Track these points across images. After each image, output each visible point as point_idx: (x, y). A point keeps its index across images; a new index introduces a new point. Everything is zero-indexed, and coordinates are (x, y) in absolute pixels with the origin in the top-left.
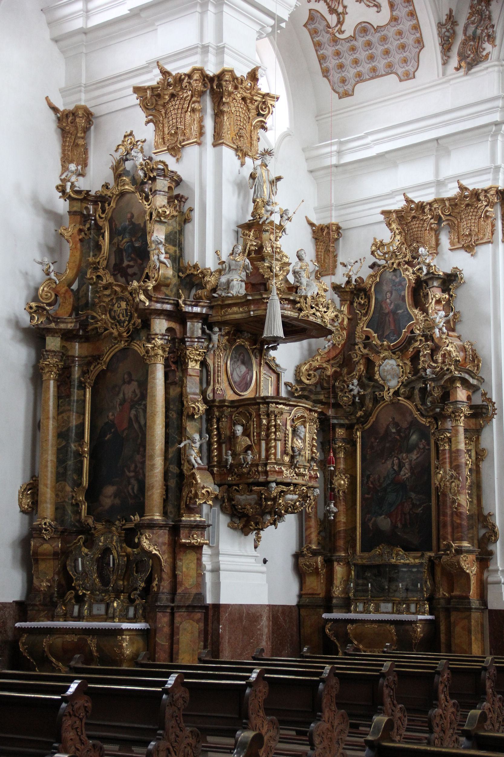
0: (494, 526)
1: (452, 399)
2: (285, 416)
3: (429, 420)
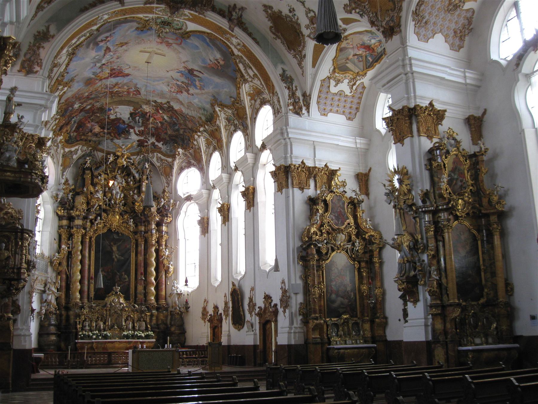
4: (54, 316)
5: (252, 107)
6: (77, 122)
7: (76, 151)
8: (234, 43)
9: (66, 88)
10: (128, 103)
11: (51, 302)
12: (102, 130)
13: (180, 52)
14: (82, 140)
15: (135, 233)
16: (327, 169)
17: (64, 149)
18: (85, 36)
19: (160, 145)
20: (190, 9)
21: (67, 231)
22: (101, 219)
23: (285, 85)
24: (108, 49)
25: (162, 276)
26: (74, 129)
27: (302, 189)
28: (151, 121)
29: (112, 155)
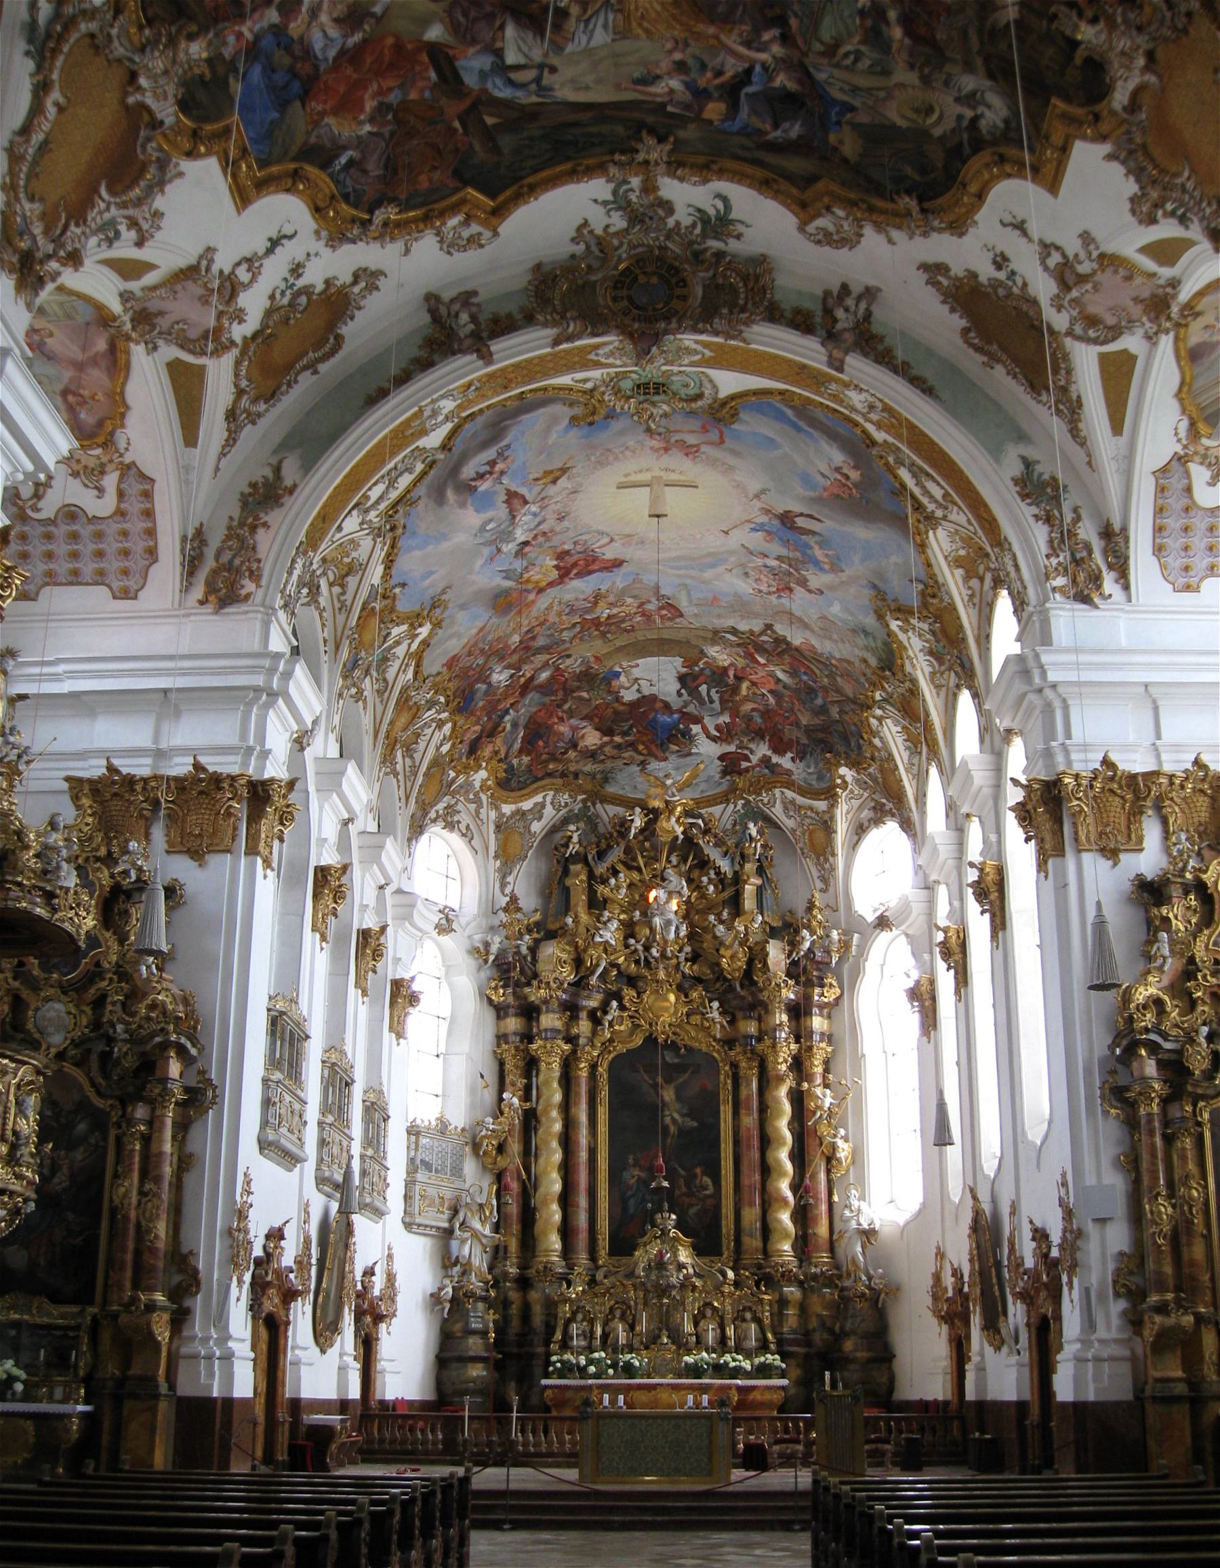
0: (196, 1272)
1: (158, 1074)
2: (8, 1078)
3: (110, 1102)
4: (480, 1305)
5: (976, 600)
6: (522, 722)
7: (539, 809)
8: (859, 406)
9: (424, 631)
10: (662, 647)
11: (469, 1262)
12: (606, 739)
13: (731, 468)
14: (550, 775)
15: (729, 1043)
16: (1206, 775)
17: (497, 808)
18: (409, 470)
19: (785, 761)
20: (695, 330)
21: (517, 1048)
22: (622, 1007)
23: (1034, 510)
24: (513, 498)
25: (814, 1177)
26: (517, 746)
27: (1111, 854)
28: (744, 692)
29: (638, 810)
